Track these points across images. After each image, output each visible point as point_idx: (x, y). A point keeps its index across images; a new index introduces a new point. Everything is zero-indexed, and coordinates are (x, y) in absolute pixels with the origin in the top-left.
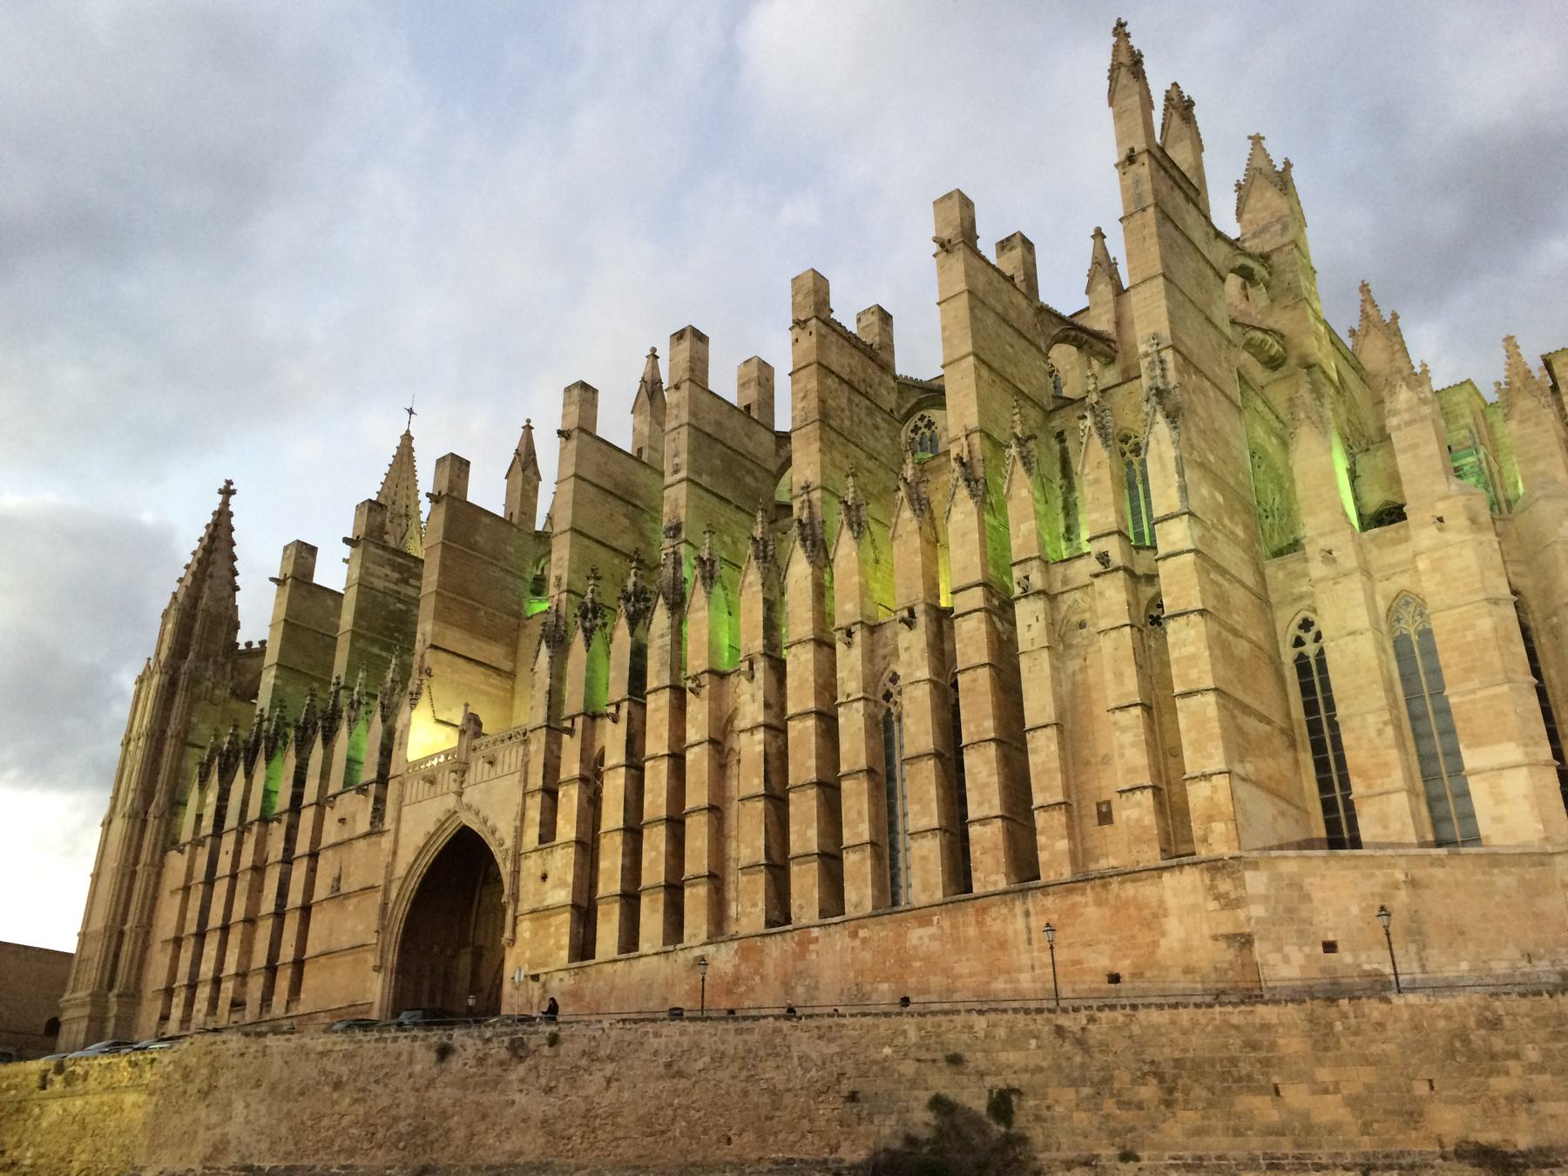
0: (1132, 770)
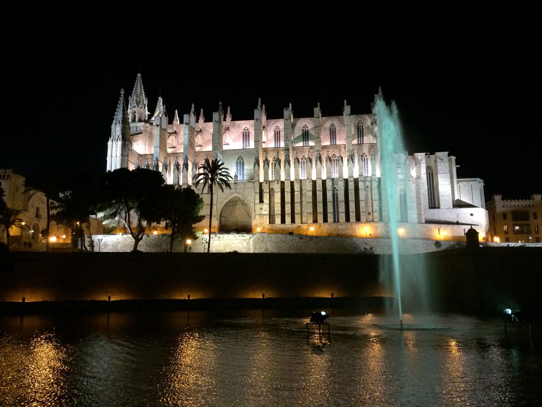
0: (375, 209)
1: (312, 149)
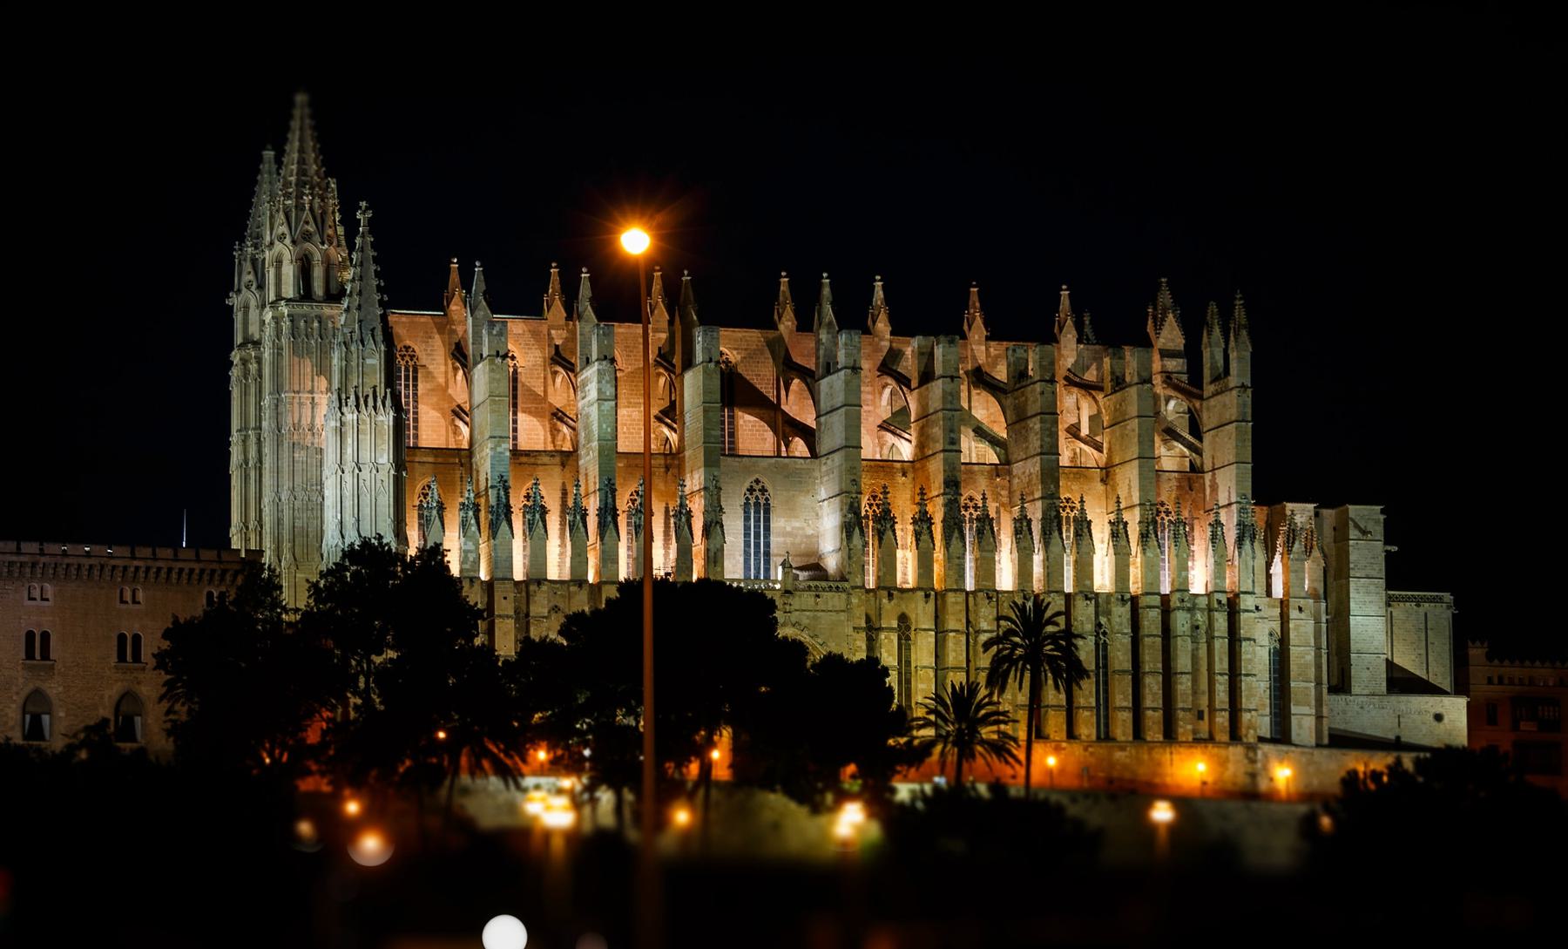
0: (1222, 702)
1: (998, 476)
